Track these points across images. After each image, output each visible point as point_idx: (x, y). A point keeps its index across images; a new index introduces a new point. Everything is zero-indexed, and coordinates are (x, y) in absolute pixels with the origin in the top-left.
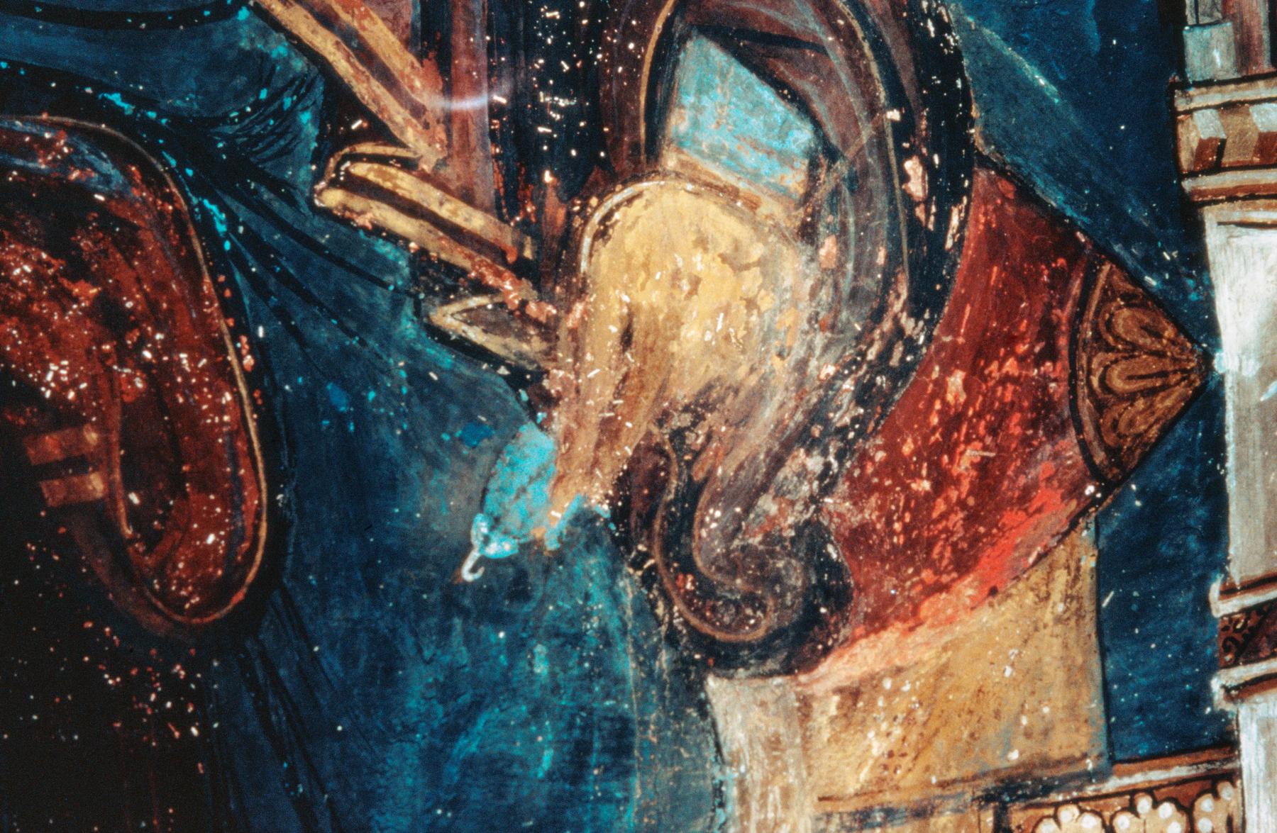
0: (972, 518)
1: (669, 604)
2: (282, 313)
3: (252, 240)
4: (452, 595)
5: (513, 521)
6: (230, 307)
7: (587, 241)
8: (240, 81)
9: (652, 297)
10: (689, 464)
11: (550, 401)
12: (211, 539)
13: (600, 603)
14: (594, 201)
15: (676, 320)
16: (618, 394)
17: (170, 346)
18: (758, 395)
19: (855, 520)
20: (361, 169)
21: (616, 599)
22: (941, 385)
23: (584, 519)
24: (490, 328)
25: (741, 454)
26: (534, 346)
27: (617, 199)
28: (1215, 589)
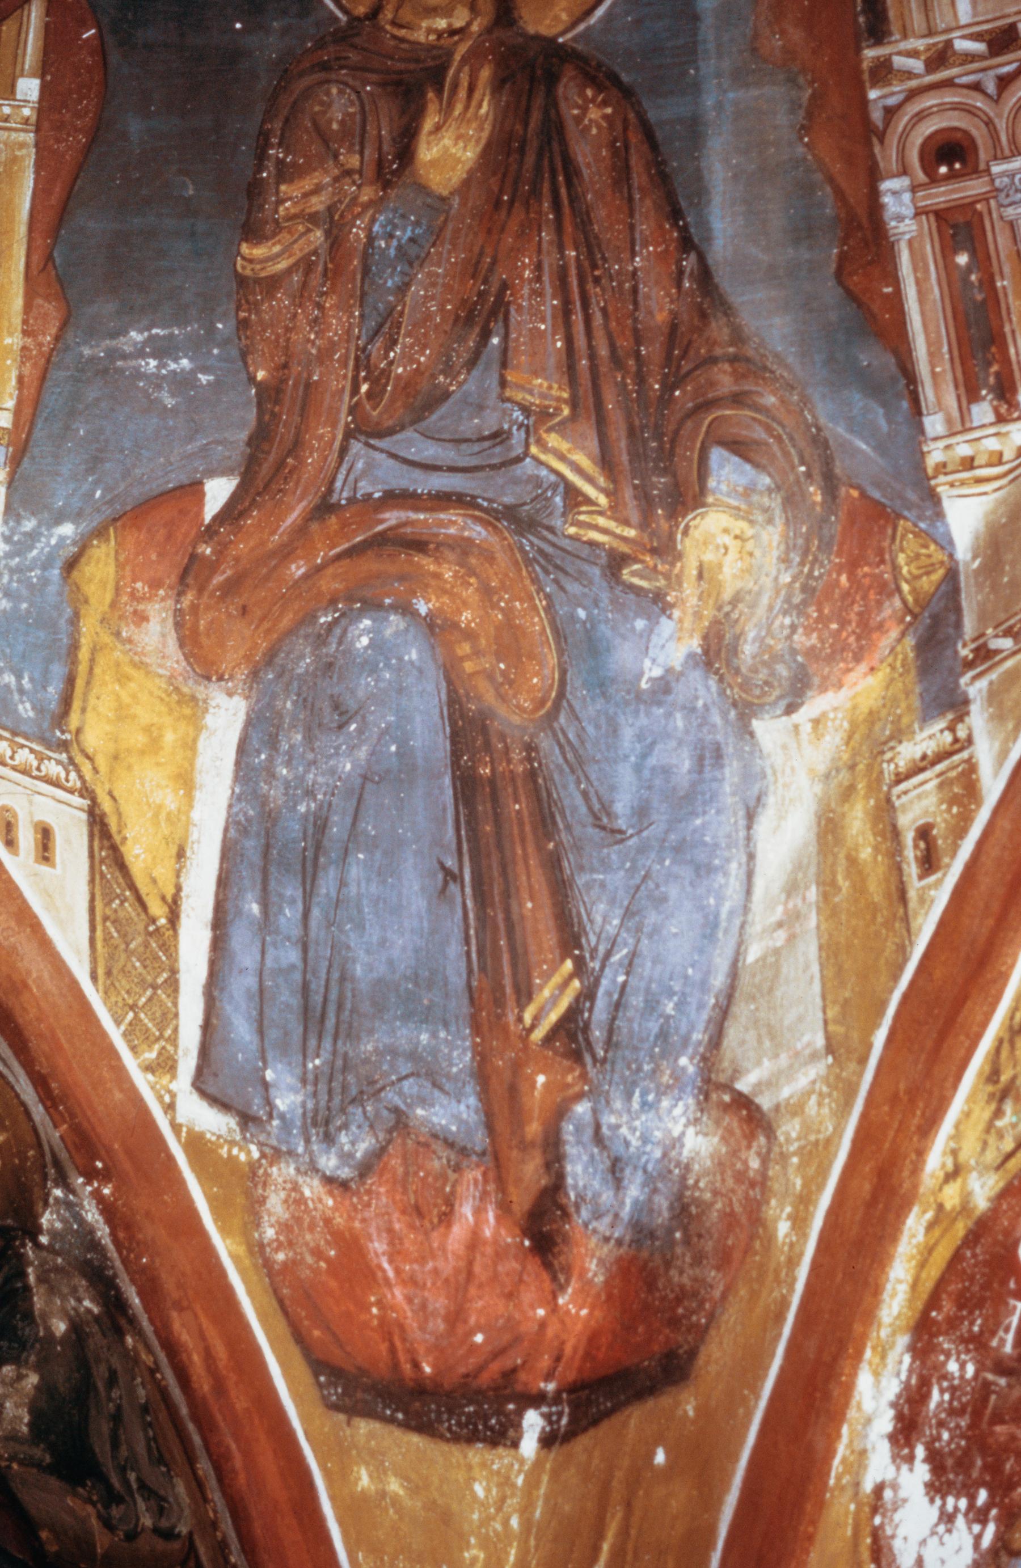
0: (858, 639)
2: (556, 581)
3: (541, 551)
4: (639, 696)
5: (661, 660)
6: (536, 580)
9: (709, 557)
11: (672, 606)
13: (702, 691)
15: (720, 566)
16: (700, 599)
18: (759, 593)
19: (808, 644)
20: (582, 518)
21: (708, 688)
22: (837, 581)
23: (691, 656)
26: (662, 583)
28: (960, 645)
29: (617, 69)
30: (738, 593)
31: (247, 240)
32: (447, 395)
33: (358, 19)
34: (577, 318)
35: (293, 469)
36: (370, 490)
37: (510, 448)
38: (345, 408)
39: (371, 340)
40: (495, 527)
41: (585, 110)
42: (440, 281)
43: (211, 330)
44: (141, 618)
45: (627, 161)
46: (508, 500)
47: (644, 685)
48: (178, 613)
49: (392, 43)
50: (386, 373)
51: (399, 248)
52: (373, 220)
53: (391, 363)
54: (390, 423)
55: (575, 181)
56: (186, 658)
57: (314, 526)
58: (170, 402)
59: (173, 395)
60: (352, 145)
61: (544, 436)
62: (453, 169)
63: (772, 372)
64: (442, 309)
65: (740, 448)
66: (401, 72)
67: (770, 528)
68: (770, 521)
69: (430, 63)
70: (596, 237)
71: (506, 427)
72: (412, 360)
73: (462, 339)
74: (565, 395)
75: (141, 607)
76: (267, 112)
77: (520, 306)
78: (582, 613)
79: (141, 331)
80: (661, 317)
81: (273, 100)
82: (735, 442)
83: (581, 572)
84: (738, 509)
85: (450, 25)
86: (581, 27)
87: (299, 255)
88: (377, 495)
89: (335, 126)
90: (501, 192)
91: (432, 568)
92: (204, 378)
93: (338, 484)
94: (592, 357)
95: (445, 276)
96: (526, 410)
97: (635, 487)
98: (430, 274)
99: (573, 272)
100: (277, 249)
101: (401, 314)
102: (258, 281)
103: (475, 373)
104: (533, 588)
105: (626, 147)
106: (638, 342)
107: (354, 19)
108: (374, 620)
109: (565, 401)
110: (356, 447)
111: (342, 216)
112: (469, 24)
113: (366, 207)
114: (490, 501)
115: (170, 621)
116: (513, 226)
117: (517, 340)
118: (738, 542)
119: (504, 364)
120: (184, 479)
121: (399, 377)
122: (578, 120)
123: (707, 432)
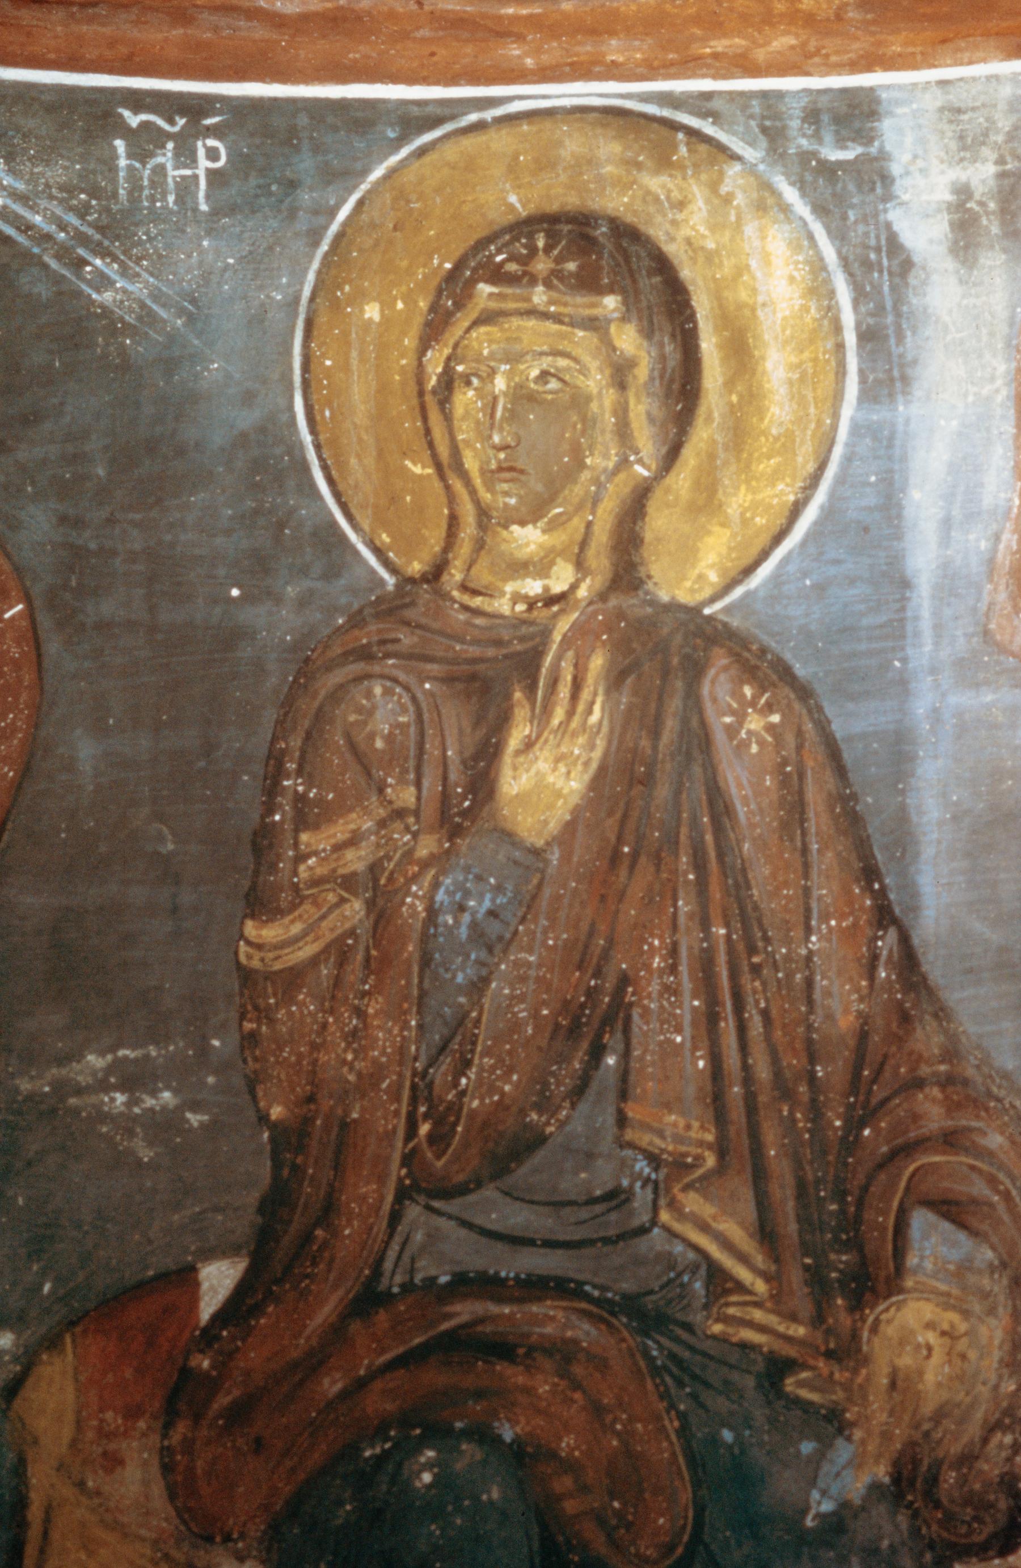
1: (929, 1527)
2: (694, 1396)
3: (673, 1356)
5: (834, 1490)
7: (865, 1334)
8: (658, 1268)
9: (906, 1361)
10: (934, 1449)
11: (853, 1424)
12: (661, 1521)
13: (888, 1528)
14: (867, 1311)
15: (921, 1373)
16: (890, 1415)
17: (631, 1420)
18: (973, 1406)
21: (897, 1526)
23: (875, 1487)
24: (813, 1389)
25: (965, 1439)
26: (839, 1395)
27: (881, 1308)
29: (788, 656)
30: (942, 1407)
31: (253, 916)
32: (541, 1140)
33: (412, 580)
34: (728, 1026)
35: (325, 1245)
36: (433, 1272)
37: (631, 1214)
38: (397, 1157)
39: (432, 1062)
40: (609, 1325)
41: (741, 717)
42: (532, 973)
43: (204, 1050)
44: (113, 1462)
45: (801, 793)
46: (627, 1286)
47: (809, 1522)
48: (166, 1454)
49: (462, 617)
50: (455, 1108)
51: (474, 925)
52: (436, 885)
53: (463, 1093)
54: (461, 1178)
55: (725, 820)
56: (179, 1515)
57: (355, 1326)
58: (146, 1154)
59: (151, 1144)
60: (407, 771)
61: (680, 1196)
62: (551, 806)
63: (999, 1100)
64: (535, 1015)
65: (951, 1209)
66: (474, 661)
67: (993, 1322)
68: (992, 1311)
69: (519, 647)
70: (756, 908)
71: (625, 1183)
72: (492, 1089)
73: (563, 1059)
74: (710, 1137)
75: (112, 1446)
76: (279, 722)
77: (646, 1010)
78: (727, 1435)
79: (102, 1054)
80: (846, 1023)
81: (288, 704)
82: (945, 1202)
83: (726, 1382)
84: (948, 1295)
85: (546, 589)
86: (738, 592)
87: (329, 937)
88: (444, 1279)
89: (379, 744)
90: (620, 840)
91: (520, 1380)
92: (194, 1119)
93: (388, 1265)
94: (748, 1078)
95: (540, 966)
96: (654, 1160)
97: (807, 1268)
98: (517, 964)
99: (722, 958)
100: (297, 928)
101: (478, 1021)
102: (270, 976)
103: (583, 1107)
104: (662, 1406)
105: (801, 776)
106: (812, 1060)
107: (407, 581)
108: (439, 1451)
109: (710, 1147)
110: (413, 1211)
111: (391, 879)
112: (574, 587)
113: (425, 865)
114: (603, 1288)
115: (155, 1462)
116: (637, 890)
117: (642, 1058)
118: (946, 1340)
119: (624, 1095)
120: (169, 1263)
121: (473, 1114)
122: (731, 731)
123: (908, 1188)
